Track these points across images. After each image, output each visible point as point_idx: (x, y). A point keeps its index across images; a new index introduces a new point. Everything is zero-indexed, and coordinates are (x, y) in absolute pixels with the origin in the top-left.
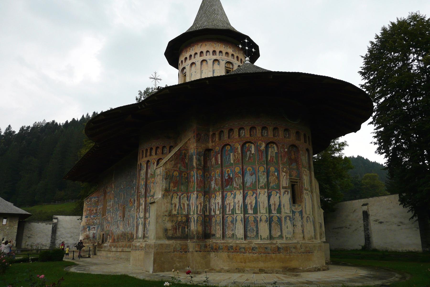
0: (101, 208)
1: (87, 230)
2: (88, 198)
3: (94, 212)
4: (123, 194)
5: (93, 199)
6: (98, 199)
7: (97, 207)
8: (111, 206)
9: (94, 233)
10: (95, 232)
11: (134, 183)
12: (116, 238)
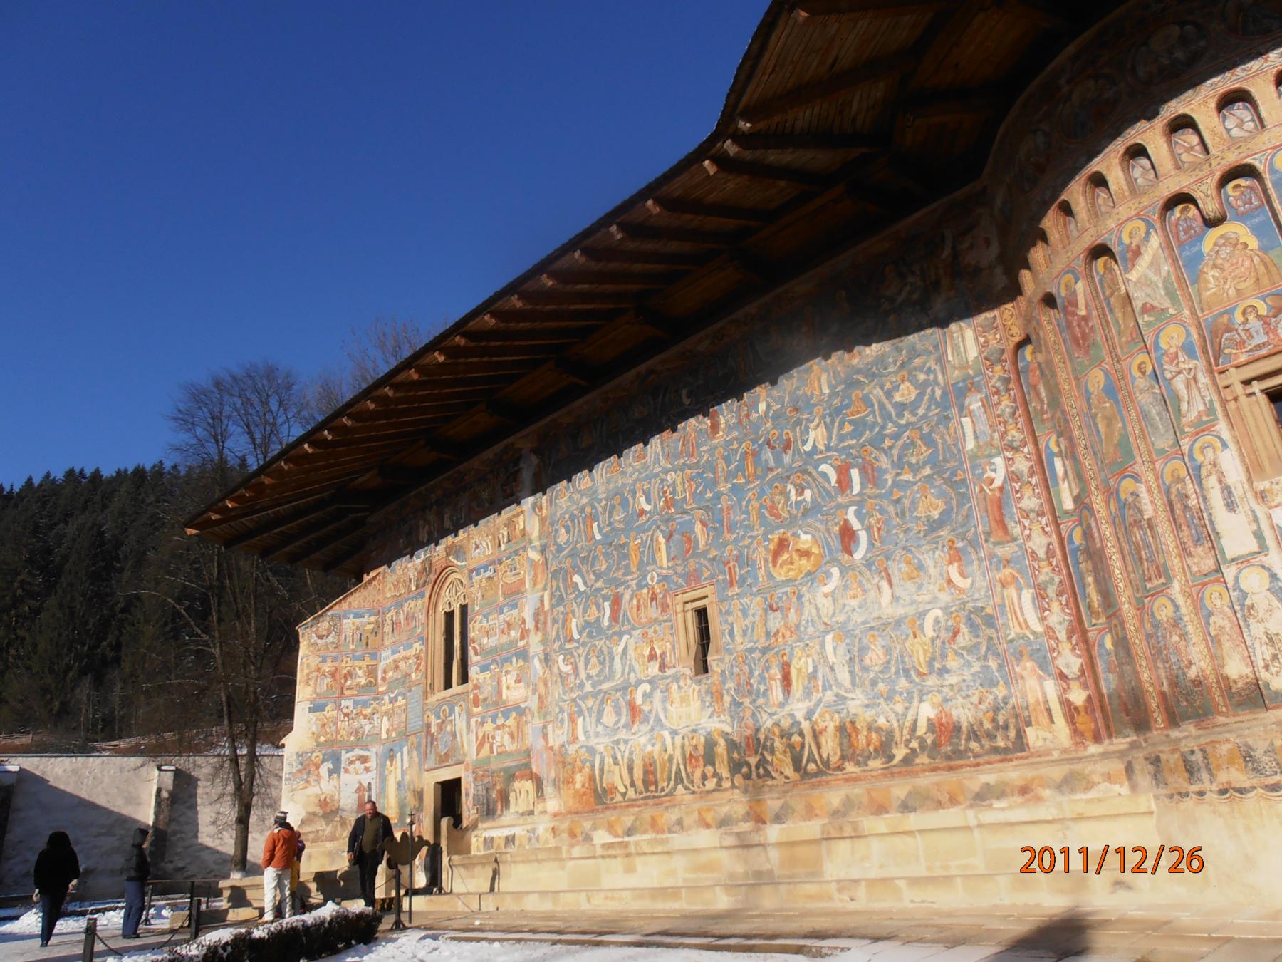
0: (406, 658)
1: (324, 770)
2: (321, 615)
3: (358, 680)
4: (669, 538)
5: (351, 619)
6: (377, 621)
7: (374, 656)
8: (530, 624)
9: (366, 785)
10: (366, 779)
11: (808, 448)
12: (617, 778)
